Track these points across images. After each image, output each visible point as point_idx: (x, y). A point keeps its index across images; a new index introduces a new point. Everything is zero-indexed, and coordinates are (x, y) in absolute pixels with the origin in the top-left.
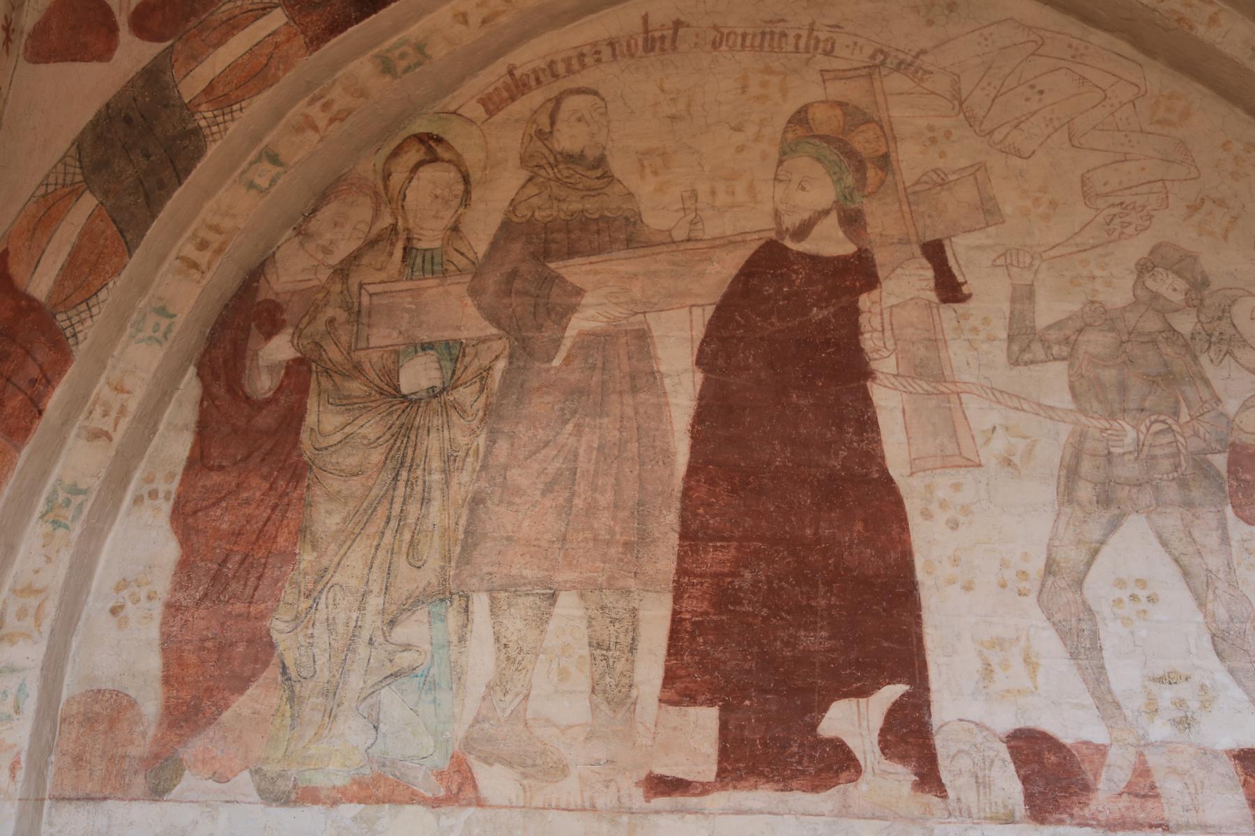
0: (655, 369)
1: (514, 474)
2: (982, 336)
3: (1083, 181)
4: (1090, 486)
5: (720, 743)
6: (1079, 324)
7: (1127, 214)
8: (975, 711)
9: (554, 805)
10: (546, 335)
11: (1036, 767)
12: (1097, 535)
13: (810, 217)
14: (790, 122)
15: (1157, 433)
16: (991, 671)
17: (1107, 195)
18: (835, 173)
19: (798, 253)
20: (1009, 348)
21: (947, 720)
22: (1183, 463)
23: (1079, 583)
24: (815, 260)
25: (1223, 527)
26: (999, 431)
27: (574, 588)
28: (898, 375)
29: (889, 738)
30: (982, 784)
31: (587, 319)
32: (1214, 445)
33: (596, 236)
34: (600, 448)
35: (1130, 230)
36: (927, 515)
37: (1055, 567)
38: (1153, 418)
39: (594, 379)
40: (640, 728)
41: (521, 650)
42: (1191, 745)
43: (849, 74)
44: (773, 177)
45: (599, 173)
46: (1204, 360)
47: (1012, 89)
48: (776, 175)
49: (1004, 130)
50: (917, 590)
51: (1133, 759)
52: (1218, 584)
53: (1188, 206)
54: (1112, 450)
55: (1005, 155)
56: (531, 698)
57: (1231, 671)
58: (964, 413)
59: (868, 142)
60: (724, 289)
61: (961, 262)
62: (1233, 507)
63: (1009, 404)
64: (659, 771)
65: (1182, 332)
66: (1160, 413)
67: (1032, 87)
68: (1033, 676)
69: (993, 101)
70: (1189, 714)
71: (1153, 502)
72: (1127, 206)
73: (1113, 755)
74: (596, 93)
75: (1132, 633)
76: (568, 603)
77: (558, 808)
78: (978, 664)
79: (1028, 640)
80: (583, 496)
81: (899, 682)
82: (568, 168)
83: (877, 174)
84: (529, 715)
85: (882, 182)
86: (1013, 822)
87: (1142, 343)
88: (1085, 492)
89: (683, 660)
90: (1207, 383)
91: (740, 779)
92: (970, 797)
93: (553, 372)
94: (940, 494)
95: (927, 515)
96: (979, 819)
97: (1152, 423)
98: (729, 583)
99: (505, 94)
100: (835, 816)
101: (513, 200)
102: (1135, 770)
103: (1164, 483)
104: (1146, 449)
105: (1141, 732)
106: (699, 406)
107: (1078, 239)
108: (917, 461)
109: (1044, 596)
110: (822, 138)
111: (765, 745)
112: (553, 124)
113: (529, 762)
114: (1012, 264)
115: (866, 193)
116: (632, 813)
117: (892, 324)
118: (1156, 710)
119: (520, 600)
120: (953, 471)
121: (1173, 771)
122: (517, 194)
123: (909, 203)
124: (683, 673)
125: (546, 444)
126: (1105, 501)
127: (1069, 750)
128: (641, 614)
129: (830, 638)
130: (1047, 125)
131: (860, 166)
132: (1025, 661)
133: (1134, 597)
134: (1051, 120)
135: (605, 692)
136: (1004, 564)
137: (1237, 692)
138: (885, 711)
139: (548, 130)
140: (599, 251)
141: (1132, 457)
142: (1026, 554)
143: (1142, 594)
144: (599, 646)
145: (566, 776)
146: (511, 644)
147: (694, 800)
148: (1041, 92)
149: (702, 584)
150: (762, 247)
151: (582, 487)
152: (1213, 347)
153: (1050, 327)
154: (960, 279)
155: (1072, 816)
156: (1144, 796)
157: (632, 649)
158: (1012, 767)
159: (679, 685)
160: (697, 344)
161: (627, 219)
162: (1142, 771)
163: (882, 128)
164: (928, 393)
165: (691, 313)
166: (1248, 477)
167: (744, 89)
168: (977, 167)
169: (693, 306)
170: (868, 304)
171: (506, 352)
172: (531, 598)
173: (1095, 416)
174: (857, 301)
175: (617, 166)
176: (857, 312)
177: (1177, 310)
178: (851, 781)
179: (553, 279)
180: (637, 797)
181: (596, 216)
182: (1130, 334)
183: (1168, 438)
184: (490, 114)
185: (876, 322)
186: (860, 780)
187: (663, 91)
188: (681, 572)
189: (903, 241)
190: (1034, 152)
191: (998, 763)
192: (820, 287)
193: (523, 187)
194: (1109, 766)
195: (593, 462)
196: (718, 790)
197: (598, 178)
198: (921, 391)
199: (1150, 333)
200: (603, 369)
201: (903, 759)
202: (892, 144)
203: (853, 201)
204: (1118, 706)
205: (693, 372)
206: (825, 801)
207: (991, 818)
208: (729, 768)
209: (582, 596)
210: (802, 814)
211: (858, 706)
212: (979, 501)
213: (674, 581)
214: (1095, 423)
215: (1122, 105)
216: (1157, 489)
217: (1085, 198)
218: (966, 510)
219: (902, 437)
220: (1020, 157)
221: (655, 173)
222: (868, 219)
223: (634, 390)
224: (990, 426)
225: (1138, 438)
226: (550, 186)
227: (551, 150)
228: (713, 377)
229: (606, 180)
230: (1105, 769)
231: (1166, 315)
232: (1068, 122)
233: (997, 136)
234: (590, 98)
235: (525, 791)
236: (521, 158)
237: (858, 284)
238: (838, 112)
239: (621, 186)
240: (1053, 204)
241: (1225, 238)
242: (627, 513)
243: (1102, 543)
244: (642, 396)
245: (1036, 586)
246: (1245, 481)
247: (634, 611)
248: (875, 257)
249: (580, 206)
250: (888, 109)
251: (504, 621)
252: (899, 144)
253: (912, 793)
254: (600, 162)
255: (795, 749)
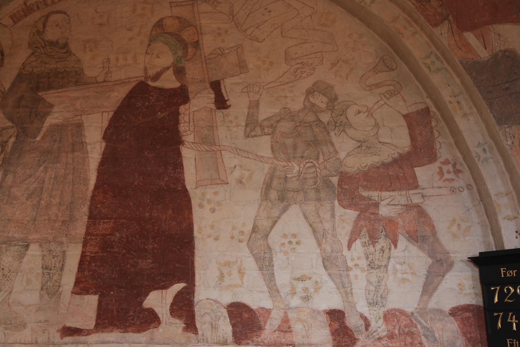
0: (84, 141)
1: (15, 191)
2: (234, 124)
3: (286, 53)
4: (275, 192)
5: (98, 311)
6: (278, 118)
7: (304, 68)
8: (214, 294)
9: (18, 341)
10: (35, 126)
11: (239, 320)
12: (277, 215)
13: (161, 71)
14: (154, 26)
15: (308, 167)
16: (223, 277)
17: (296, 59)
18: (173, 50)
19: (154, 87)
20: (245, 129)
21: (201, 299)
22: (319, 181)
23: (267, 236)
24: (161, 90)
25: (333, 210)
26: (238, 168)
27: (37, 242)
28: (194, 143)
29: (174, 307)
30: (214, 327)
31: (54, 119)
32: (333, 173)
33: (61, 80)
34: (56, 177)
35: (304, 75)
36: (201, 206)
37: (256, 229)
38: (307, 161)
39: (55, 146)
40: (62, 305)
41: (10, 271)
42: (308, 308)
43: (183, 4)
44: (145, 52)
45: (65, 50)
46: (332, 134)
47: (257, 10)
48: (147, 51)
49: (252, 29)
50: (193, 240)
51: (282, 315)
52: (328, 236)
53: (331, 64)
54: (287, 175)
55: (251, 41)
56: (12, 293)
57: (330, 275)
58: (222, 159)
59: (190, 35)
60: (119, 104)
61: (227, 91)
62: (338, 201)
63: (244, 155)
64: (68, 324)
65: (324, 122)
66: (310, 159)
67: (266, 9)
68: (242, 279)
69: (248, 16)
70: (309, 294)
71: (303, 199)
72: (304, 64)
73: (273, 314)
74: (65, 13)
75: (288, 258)
76: (34, 250)
77: (20, 343)
78: (218, 273)
79: (241, 262)
80: (46, 200)
81: (182, 282)
82: (51, 48)
83: (193, 50)
84: (11, 301)
85: (195, 54)
86: (227, 345)
87: (305, 126)
88: (273, 195)
89: (84, 274)
90: (332, 144)
91: (106, 327)
92: (208, 334)
93: (36, 143)
94: (208, 196)
95: (201, 206)
96: (211, 343)
97: (306, 163)
98: (109, 238)
99: (22, 14)
100: (147, 343)
101: (23, 63)
102: (282, 320)
103: (309, 190)
104: (302, 175)
105: (287, 303)
106: (103, 158)
107: (281, 79)
108: (199, 182)
109: (251, 242)
110: (169, 33)
111: (118, 312)
112: (44, 27)
113: (8, 322)
114: (250, 91)
115: (187, 59)
116: (54, 344)
117: (193, 120)
118: (295, 293)
119: (11, 248)
120: (215, 186)
121: (299, 320)
122: (26, 60)
123: (206, 63)
124: (84, 280)
125: (31, 176)
126: (282, 199)
127: (254, 312)
128: (67, 253)
129: (152, 263)
130: (271, 27)
131: (185, 47)
132: (239, 272)
133: (290, 242)
134: (274, 24)
135: (47, 289)
136: (234, 228)
137: (331, 284)
138: (174, 295)
139: (42, 31)
140: (62, 87)
141: (296, 179)
142: (244, 223)
143: (294, 241)
144: (46, 268)
145: (25, 328)
146: (5, 268)
147: (84, 338)
148: (270, 11)
149: (96, 239)
150: (138, 84)
151: (45, 195)
152: (337, 128)
153: (265, 120)
154: (226, 98)
155: (253, 341)
156: (285, 332)
157: (62, 269)
158: (228, 320)
159: (82, 285)
160: (104, 129)
161: (76, 72)
162: (286, 320)
163: (196, 29)
164: (207, 151)
165: (102, 115)
166: (347, 187)
167: (134, 11)
168: (238, 47)
169: (104, 112)
170: (184, 110)
171: (15, 134)
172: (17, 247)
173: (281, 160)
174: (179, 109)
175: (73, 47)
176: (178, 114)
177: (322, 112)
178: (155, 328)
179: (41, 100)
180: (57, 337)
181: (62, 71)
182: (300, 122)
183: (313, 170)
184: (15, 23)
185: (186, 118)
186: (160, 327)
187: (96, 12)
188: (87, 234)
189: (202, 81)
190: (264, 39)
191: (222, 318)
192: (162, 103)
193: (29, 57)
194: (271, 318)
195: (51, 184)
196: (95, 333)
197: (64, 53)
198: (204, 150)
199: (309, 122)
200: (60, 141)
201: (180, 317)
202: (200, 36)
203: (181, 63)
204: (278, 291)
205: (101, 142)
206: (143, 337)
207: (217, 343)
208: (101, 323)
209: (40, 246)
210: (132, 343)
211: (162, 294)
212: (225, 199)
213: (84, 238)
214: (281, 163)
215: (306, 17)
216: (306, 193)
217: (286, 60)
218: (219, 204)
219: (194, 171)
220: (258, 42)
221: (91, 51)
222: (187, 71)
223: (73, 151)
224: (233, 165)
225: (300, 170)
226: (42, 57)
227: (43, 40)
228: (110, 144)
229: (67, 54)
230: (269, 320)
231: (317, 114)
232: (281, 25)
233: (248, 32)
234: (62, 15)
235: (5, 336)
236: (29, 44)
237: (179, 101)
238: (177, 21)
239: (75, 57)
240: (271, 63)
241: (347, 78)
242: (65, 207)
243: (279, 218)
244: (77, 154)
245: (248, 237)
246: (346, 189)
247: (64, 253)
248: (189, 88)
249: (55, 66)
250: (200, 20)
251: (3, 258)
252: (203, 36)
253: (183, 332)
254: (66, 45)
255: (131, 314)
